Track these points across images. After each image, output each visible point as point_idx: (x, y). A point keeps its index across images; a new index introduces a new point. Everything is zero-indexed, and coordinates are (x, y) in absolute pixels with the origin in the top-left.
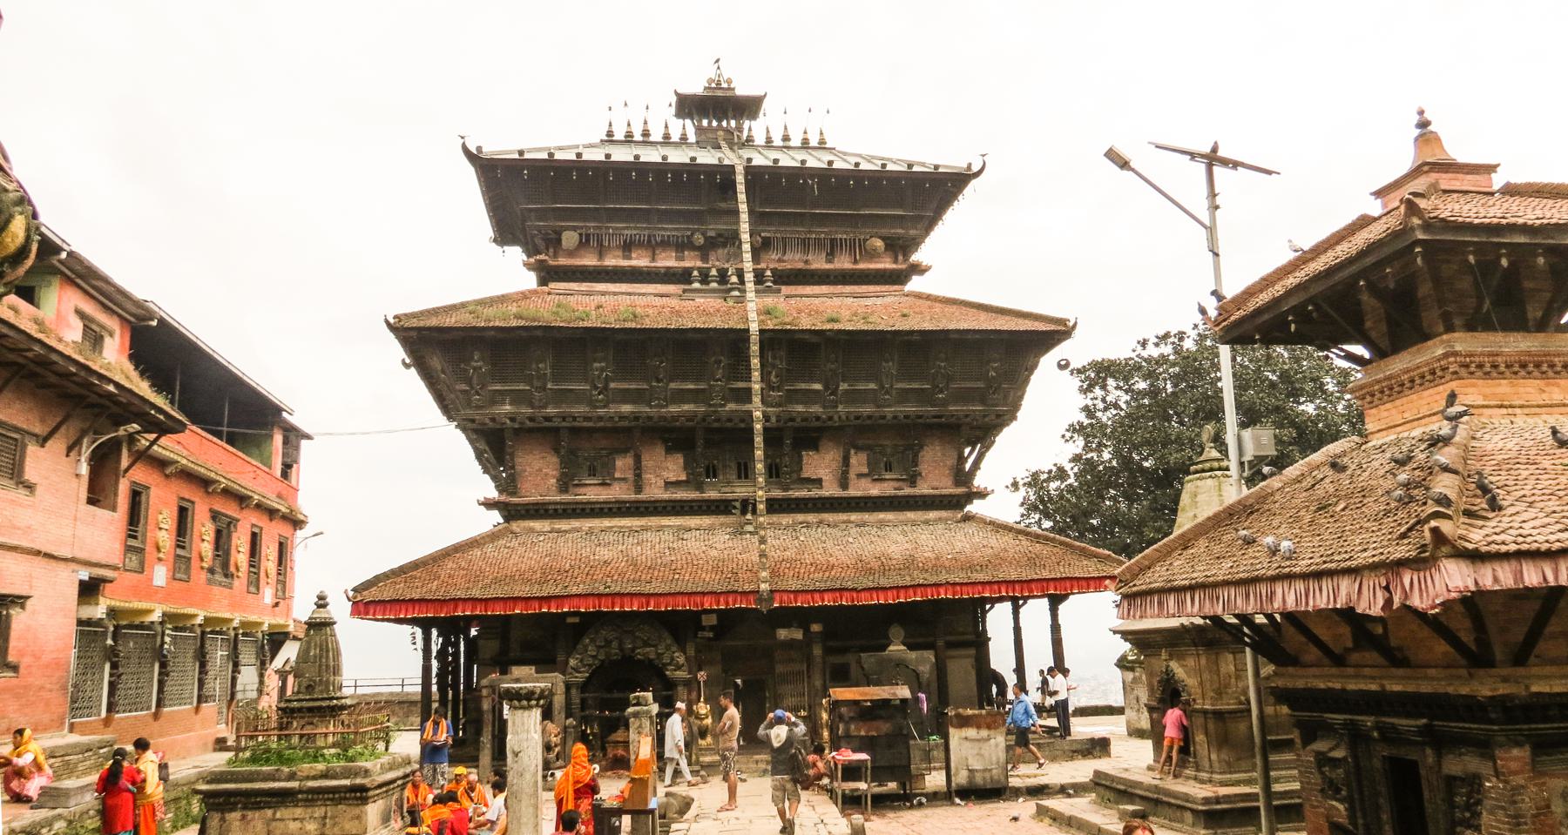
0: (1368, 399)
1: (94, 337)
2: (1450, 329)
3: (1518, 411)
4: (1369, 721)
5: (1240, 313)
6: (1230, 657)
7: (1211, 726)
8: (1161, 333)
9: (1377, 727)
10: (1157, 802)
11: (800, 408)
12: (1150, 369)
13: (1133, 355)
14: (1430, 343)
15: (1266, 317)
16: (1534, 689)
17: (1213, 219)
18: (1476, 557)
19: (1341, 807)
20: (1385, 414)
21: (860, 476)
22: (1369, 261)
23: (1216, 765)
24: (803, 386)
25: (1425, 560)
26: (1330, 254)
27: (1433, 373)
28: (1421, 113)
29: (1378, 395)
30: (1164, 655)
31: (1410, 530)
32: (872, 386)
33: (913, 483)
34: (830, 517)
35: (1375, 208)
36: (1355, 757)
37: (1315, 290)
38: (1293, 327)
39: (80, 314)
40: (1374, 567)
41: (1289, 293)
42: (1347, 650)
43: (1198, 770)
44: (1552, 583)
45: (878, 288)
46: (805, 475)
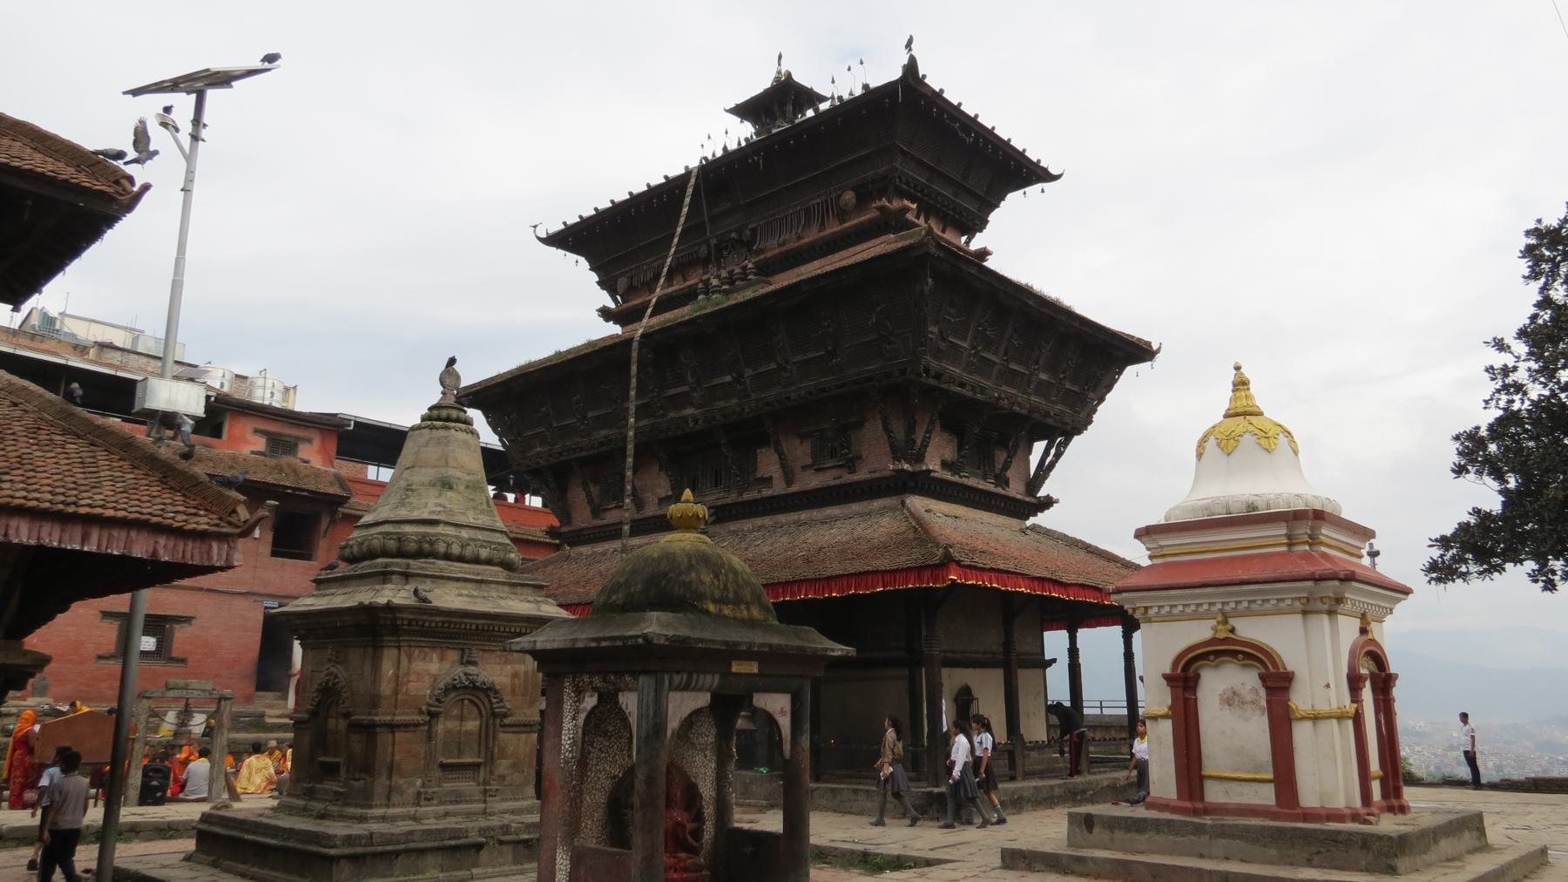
1: (278, 445)
11: (722, 404)
17: (193, 149)
21: (805, 468)
24: (716, 381)
32: (773, 366)
33: (851, 464)
34: (782, 518)
39: (256, 431)
45: (865, 246)
46: (759, 475)
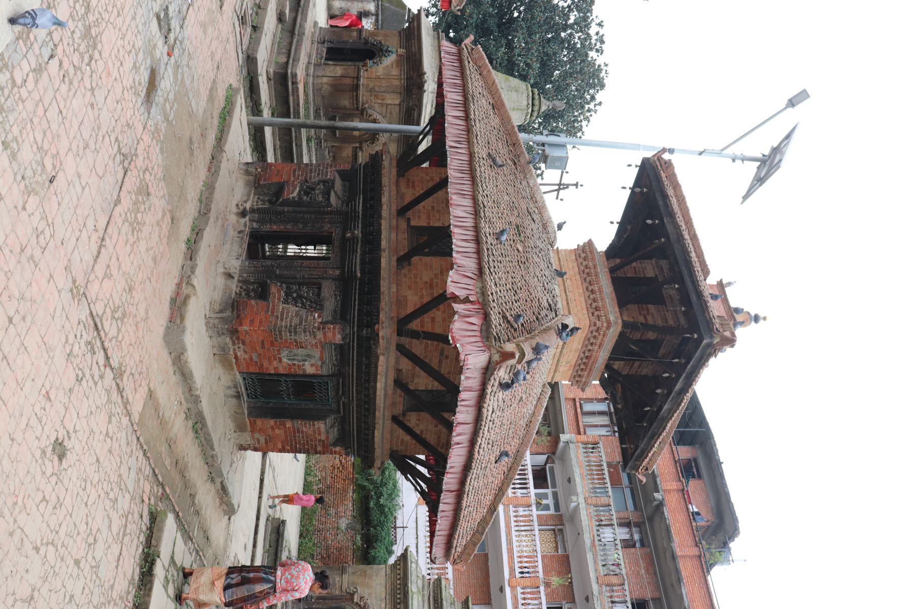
0: (583, 255)
2: (625, 325)
3: (559, 350)
4: (358, 233)
5: (664, 179)
6: (397, 102)
7: (348, 81)
8: (605, 38)
9: (354, 239)
10: (292, 33)
12: (583, 24)
13: (594, 17)
14: (617, 309)
15: (661, 203)
16: (382, 358)
17: (727, 156)
18: (488, 371)
19: (295, 194)
20: (571, 266)
22: (694, 298)
23: (319, 81)
25: (488, 338)
26: (698, 264)
27: (597, 309)
28: (765, 319)
29: (584, 263)
30: (402, 51)
31: (508, 322)
35: (712, 280)
36: (331, 213)
37: (677, 247)
38: (649, 222)
40: (483, 292)
41: (677, 227)
42: (409, 220)
43: (315, 65)
44: (459, 403)
